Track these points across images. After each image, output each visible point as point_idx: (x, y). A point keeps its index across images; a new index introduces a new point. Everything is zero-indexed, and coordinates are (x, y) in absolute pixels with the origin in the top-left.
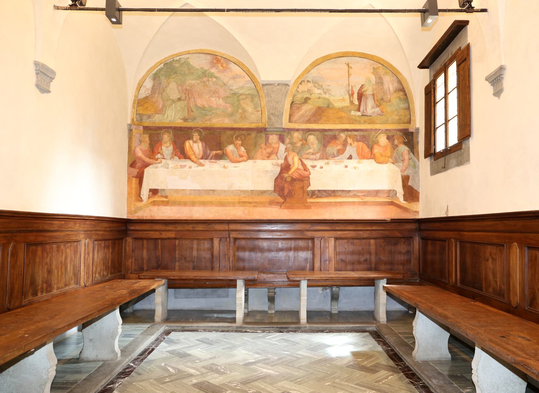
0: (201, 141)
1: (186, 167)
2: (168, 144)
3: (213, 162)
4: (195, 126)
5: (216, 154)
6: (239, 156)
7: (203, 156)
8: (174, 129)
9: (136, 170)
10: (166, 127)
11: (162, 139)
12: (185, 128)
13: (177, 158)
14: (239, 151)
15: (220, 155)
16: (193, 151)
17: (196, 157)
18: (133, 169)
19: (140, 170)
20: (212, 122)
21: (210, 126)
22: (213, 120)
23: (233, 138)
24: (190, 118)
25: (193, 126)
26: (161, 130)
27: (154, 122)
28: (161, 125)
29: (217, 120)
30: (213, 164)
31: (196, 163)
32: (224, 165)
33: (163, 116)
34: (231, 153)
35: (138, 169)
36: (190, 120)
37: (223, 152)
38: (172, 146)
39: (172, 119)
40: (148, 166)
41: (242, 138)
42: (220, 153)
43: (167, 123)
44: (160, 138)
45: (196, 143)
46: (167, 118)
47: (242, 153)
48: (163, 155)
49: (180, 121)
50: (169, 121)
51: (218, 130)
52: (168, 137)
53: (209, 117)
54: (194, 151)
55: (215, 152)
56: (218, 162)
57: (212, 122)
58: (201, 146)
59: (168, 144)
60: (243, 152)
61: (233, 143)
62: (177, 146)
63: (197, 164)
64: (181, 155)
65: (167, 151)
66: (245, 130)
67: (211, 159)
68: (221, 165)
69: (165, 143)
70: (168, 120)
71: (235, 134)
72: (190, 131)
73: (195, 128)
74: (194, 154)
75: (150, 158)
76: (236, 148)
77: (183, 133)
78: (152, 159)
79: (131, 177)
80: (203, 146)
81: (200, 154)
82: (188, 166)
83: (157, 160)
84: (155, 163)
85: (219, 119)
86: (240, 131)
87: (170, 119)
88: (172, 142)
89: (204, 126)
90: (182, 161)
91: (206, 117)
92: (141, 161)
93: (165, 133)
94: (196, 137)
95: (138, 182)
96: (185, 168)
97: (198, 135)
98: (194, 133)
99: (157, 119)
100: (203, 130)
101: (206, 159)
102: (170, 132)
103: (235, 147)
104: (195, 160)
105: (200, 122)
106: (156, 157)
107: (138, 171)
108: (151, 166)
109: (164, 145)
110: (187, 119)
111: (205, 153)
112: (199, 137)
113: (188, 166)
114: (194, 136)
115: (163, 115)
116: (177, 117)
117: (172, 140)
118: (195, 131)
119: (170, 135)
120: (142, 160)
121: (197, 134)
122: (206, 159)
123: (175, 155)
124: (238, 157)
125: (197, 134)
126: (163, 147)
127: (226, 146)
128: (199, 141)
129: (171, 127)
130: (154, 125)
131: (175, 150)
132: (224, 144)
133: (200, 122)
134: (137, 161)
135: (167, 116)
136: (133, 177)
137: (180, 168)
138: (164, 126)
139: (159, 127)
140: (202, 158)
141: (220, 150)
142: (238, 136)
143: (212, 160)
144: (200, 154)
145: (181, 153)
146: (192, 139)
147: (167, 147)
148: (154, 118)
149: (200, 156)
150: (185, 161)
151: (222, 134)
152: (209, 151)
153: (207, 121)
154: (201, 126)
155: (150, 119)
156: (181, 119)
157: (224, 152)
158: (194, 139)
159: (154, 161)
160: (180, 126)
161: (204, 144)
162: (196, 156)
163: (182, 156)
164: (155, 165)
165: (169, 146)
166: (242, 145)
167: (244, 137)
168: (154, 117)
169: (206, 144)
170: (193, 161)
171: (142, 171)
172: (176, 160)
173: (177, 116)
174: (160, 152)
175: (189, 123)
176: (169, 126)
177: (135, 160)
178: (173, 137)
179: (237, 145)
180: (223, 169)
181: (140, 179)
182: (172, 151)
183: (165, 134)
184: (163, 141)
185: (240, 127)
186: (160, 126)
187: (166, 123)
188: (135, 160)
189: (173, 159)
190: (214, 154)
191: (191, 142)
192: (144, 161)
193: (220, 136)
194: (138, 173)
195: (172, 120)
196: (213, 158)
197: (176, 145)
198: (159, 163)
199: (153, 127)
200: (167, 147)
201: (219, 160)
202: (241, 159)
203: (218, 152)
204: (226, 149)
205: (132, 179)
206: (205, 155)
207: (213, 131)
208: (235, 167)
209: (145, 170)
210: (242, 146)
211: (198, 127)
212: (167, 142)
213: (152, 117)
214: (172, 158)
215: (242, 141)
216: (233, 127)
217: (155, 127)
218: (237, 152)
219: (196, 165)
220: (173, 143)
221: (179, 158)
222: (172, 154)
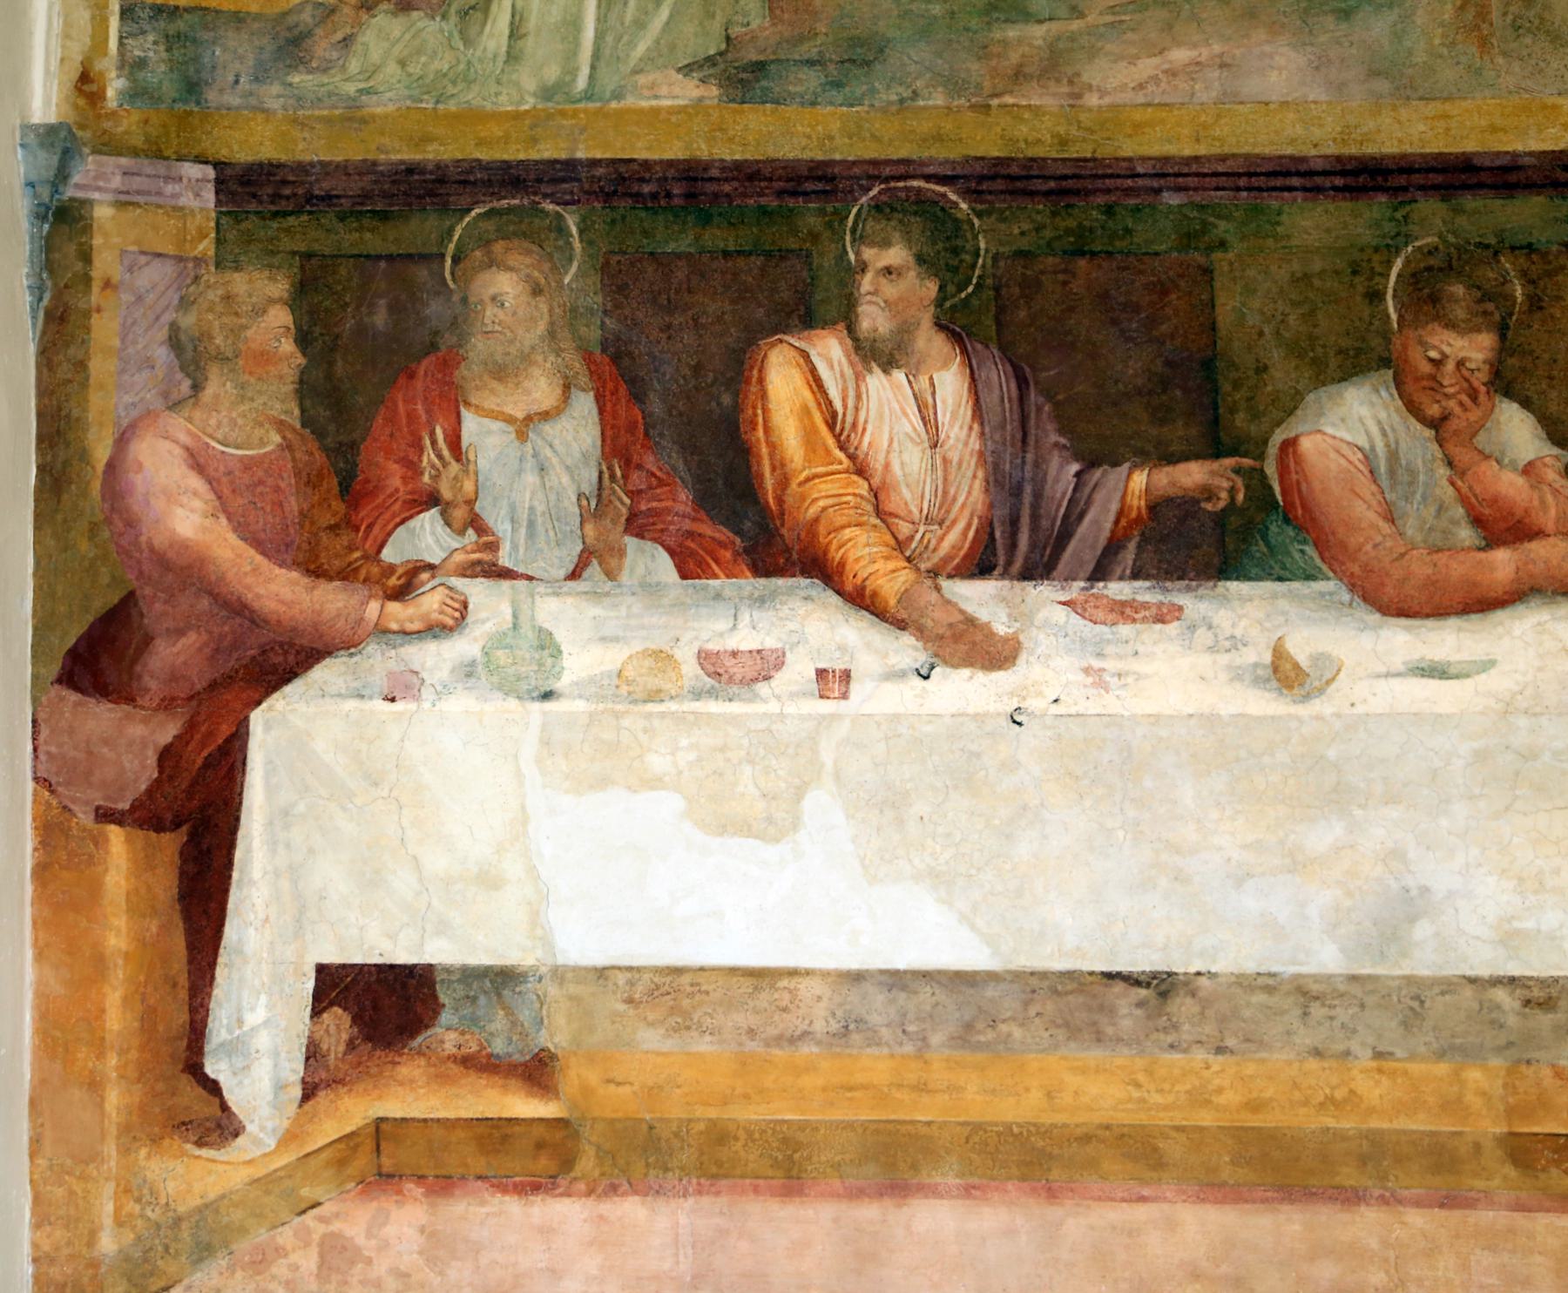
0: (956, 338)
1: (781, 680)
2: (540, 390)
3: (1124, 611)
4: (870, 152)
5: (1157, 506)
6: (1477, 521)
7: (987, 528)
8: (607, 197)
9: (137, 730)
10: (507, 165)
11: (460, 323)
12: (748, 174)
13: (663, 565)
14: (1462, 456)
15: (1220, 519)
16: (861, 471)
17: (900, 545)
18: (100, 716)
19: (191, 726)
20: (1092, 100)
21: (1063, 142)
22: (1092, 74)
23: (1376, 296)
24: (809, 50)
25: (844, 150)
26: (444, 208)
27: (353, 117)
28: (443, 150)
29: (1147, 66)
30: (1125, 630)
31: (901, 625)
32: (1279, 653)
33: (468, 42)
34: (1366, 487)
35: (167, 705)
36: (811, 80)
37: (1256, 479)
38: (584, 404)
39: (573, 72)
40: (286, 676)
41: (1490, 297)
42: (1209, 493)
43: (517, 116)
44: (434, 309)
45: (888, 365)
46: (513, 57)
47: (1510, 486)
48: (476, 523)
49: (682, 91)
50: (547, 93)
51: (1172, 199)
52: (537, 291)
53: (1038, 33)
54: (877, 464)
55: (1139, 480)
56: (1196, 603)
57: (1092, 100)
58: (966, 412)
59: (540, 390)
60: (1528, 470)
61: (1385, 362)
62: (656, 406)
63: (921, 632)
64: (707, 529)
65: (531, 478)
66: (1531, 187)
67: (1100, 572)
68: (1235, 643)
69: (500, 372)
70: (530, 84)
71: (1409, 238)
72: (810, 216)
73: (874, 171)
74: (880, 506)
75: (316, 572)
76: (1436, 424)
77: (718, 237)
78: (346, 575)
79: (85, 818)
80: (991, 399)
81: (946, 500)
82: (800, 670)
83: (401, 593)
84: (381, 631)
85: (1180, 55)
86: (1470, 202)
87: (552, 73)
88: (588, 358)
89: (986, 141)
90: (718, 596)
91: (1012, 33)
92: (205, 603)
93: (498, 247)
94: (890, 290)
95: (165, 883)
96: (762, 688)
97: (921, 259)
98: (859, 239)
99: (392, 69)
100: (972, 194)
101: (1038, 569)
102: (561, 230)
103: (1413, 408)
104: (891, 579)
105: (939, 99)
106: (389, 555)
107: (168, 732)
108: (324, 673)
109: (490, 403)
110: (759, 67)
111: (1017, 491)
112: (932, 288)
113: (800, 670)
114: (867, 283)
115: (464, 14)
116: (641, 49)
117: (594, 334)
118: (878, 207)
119: (558, 271)
120: (215, 596)
121: (896, 255)
122: (1027, 575)
123: (637, 525)
124: (1466, 534)
125: (896, 255)
126: (471, 425)
127: (1289, 406)
128: (930, 342)
129: (571, 164)
130: (351, 150)
131: (627, 464)
132: (1262, 369)
133: (939, 99)
134: (155, 611)
135: (515, 33)
136: (106, 816)
137: (697, 695)
138: (483, 155)
139: (411, 169)
140: (980, 564)
141: (1215, 446)
142: (1449, 269)
143: (1117, 589)
144: (946, 500)
145: (705, 501)
146: (847, 318)
147: (524, 426)
148: (354, 66)
149: (955, 538)
150: (761, 601)
151: (1223, 245)
152: (1063, 474)
153: (1019, 76)
154: (955, 153)
155: (296, 79)
156: (687, 70)
157: (1271, 469)
158: (873, 319)
159: (373, 608)
160: (675, 151)
161: (997, 376)
162: (904, 529)
163: (723, 533)
164: (377, 661)
165: (546, 416)
166: (1504, 383)
167: (1529, 280)
168: (347, 41)
169: (1022, 383)
170: (862, 600)
171: (225, 730)
172: (650, 589)
173: (640, 25)
174: (446, 494)
175: (790, 111)
176: (548, 151)
177: (130, 598)
178: (596, 300)
179: (1434, 384)
180: (1264, 704)
181: (193, 837)
182: (589, 477)
183: (491, 263)
184: (478, 347)
185: (1470, 146)
186: (433, 153)
187: (496, 116)
188: (130, 598)
189: (611, 575)
190: (1137, 502)
191: (829, 351)
192: (239, 610)
193: (1207, 272)
194: (167, 755)
195: (581, 83)
196: (1129, 555)
197: (638, 397)
198: (435, 630)
199: (344, 169)
200: (524, 426)
201: (1206, 588)
202: (1503, 563)
203: (1192, 474)
204: (1290, 445)
205: (100, 841)
206: (1014, 522)
207: (1109, 210)
208: (1436, 671)
209: (257, 718)
210: (1508, 393)
211: (907, 168)
212: (526, 358)
213: (322, 47)
214: (594, 569)
215: (1502, 330)
216: (1370, 149)
217: (368, 167)
218: (1443, 472)
219: (906, 650)
220: (594, 372)
221: (690, 565)
222: (595, 508)
